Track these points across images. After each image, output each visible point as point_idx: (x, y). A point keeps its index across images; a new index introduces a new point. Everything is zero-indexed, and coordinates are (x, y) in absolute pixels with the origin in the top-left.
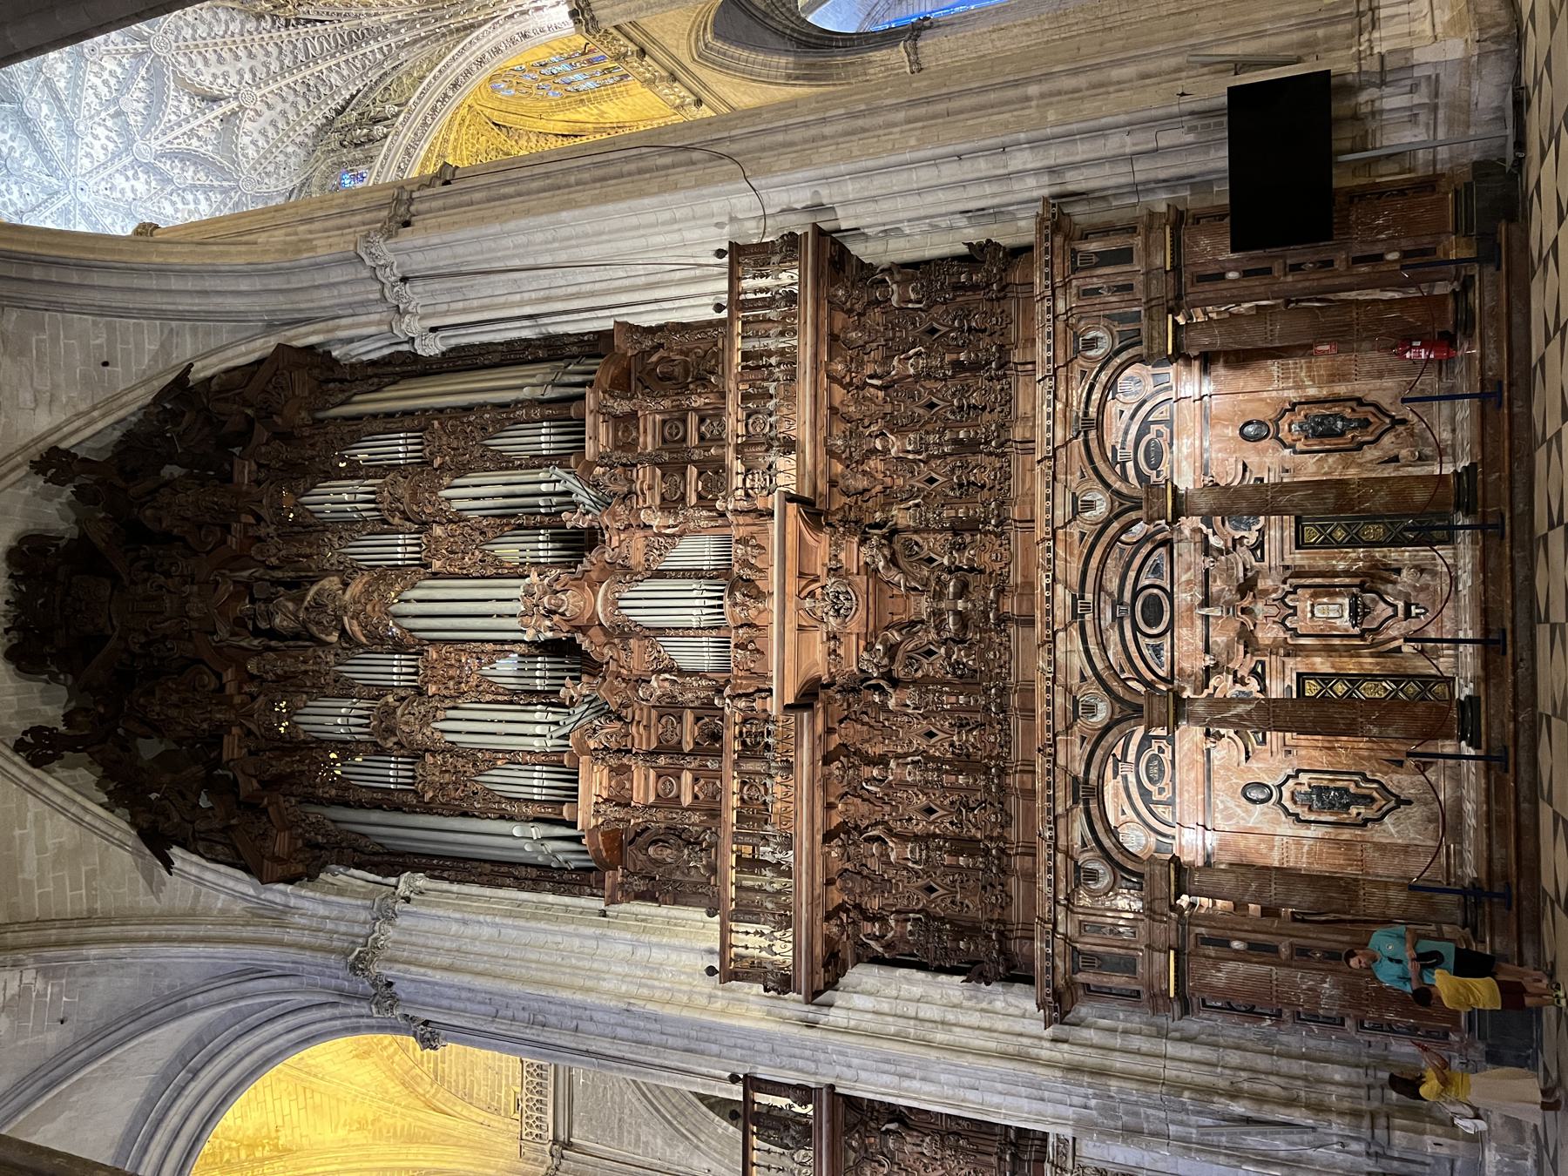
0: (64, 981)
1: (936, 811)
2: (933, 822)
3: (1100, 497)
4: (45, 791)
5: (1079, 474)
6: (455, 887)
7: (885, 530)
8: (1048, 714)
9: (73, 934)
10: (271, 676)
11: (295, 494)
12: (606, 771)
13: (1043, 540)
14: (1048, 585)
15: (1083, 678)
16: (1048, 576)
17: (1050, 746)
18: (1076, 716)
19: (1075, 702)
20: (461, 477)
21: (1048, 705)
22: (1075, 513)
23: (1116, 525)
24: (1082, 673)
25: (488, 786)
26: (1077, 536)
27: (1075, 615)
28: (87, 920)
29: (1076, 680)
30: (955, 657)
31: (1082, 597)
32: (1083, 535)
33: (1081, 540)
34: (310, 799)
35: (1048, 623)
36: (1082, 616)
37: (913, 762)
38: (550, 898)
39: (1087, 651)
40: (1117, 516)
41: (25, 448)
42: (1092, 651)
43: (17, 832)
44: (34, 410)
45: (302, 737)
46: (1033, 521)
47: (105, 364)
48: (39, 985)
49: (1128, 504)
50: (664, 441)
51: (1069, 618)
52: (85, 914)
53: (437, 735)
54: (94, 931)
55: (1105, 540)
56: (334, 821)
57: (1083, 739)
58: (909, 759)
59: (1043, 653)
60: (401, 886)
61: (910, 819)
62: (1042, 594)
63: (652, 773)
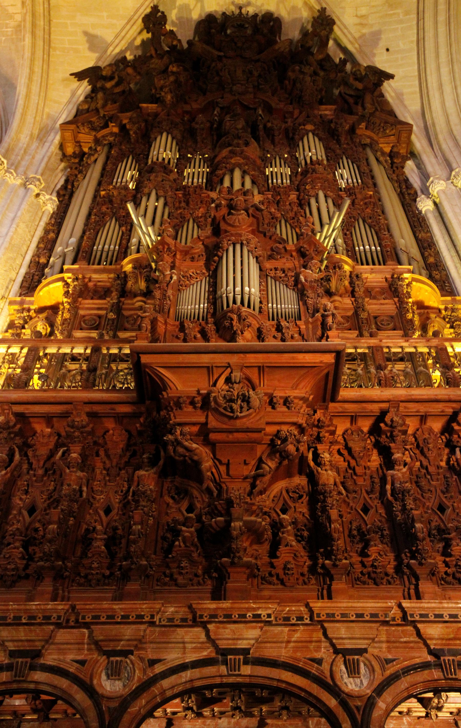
0: (14, 37)
1: (30, 516)
2: (20, 513)
3: (365, 683)
4: (128, 27)
5: (390, 657)
6: (42, 224)
7: (312, 464)
8: (112, 617)
9: (40, 33)
10: (193, 124)
11: (314, 130)
12: (108, 284)
13: (311, 611)
14: (259, 616)
15: (152, 663)
16: (269, 616)
17: (77, 621)
18: (109, 654)
19: (125, 653)
20: (334, 204)
21: (123, 617)
22: (345, 652)
23: (332, 702)
24: (159, 661)
25: (108, 224)
26: (318, 655)
27: (224, 652)
28: (48, 42)
29: (151, 655)
30: (184, 528)
31: (246, 662)
32: (319, 662)
33: (313, 660)
34: (111, 146)
35: (215, 616)
36: (225, 662)
37: (81, 491)
38: (23, 271)
39: (183, 667)
40: (344, 704)
41: (334, 12)
42: (183, 674)
43: (105, 14)
44: (356, 16)
45: (153, 136)
46: (330, 597)
47: (388, 50)
48: (12, 23)
49: (359, 717)
50: (375, 318)
51: (223, 644)
52: (52, 45)
53: (146, 190)
54: (40, 43)
55: (315, 689)
56: (96, 161)
57: (82, 663)
58: (85, 489)
59: (183, 612)
60: (48, 197)
61: (27, 492)
62: (248, 609)
63: (103, 312)
